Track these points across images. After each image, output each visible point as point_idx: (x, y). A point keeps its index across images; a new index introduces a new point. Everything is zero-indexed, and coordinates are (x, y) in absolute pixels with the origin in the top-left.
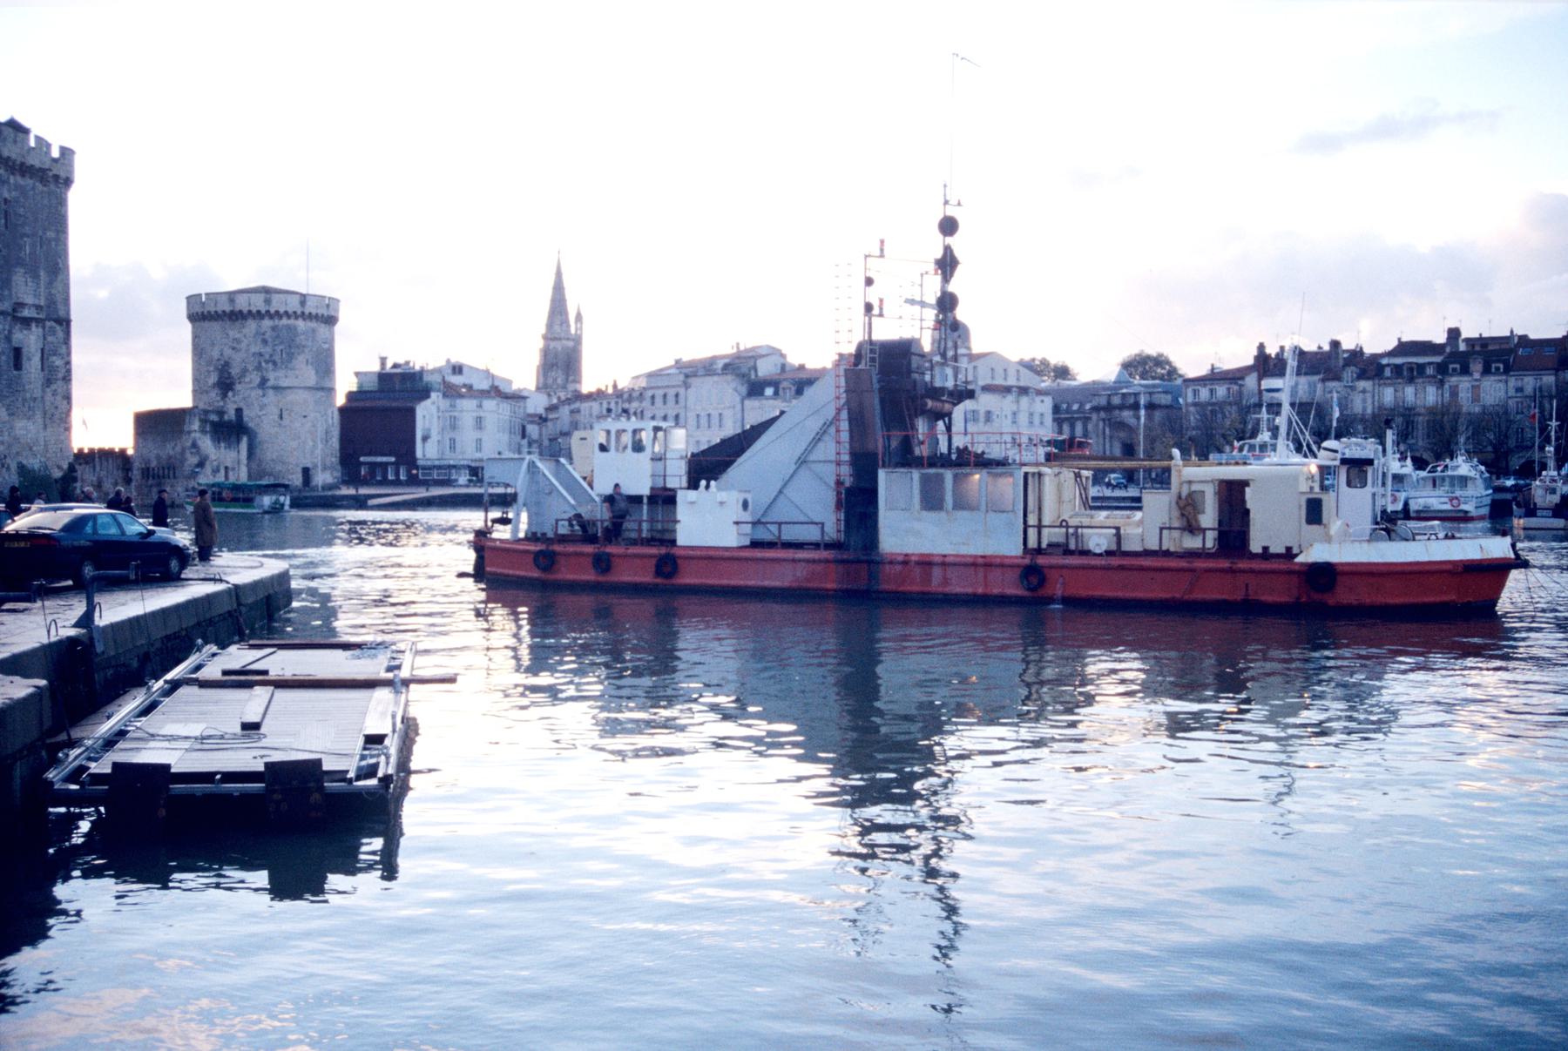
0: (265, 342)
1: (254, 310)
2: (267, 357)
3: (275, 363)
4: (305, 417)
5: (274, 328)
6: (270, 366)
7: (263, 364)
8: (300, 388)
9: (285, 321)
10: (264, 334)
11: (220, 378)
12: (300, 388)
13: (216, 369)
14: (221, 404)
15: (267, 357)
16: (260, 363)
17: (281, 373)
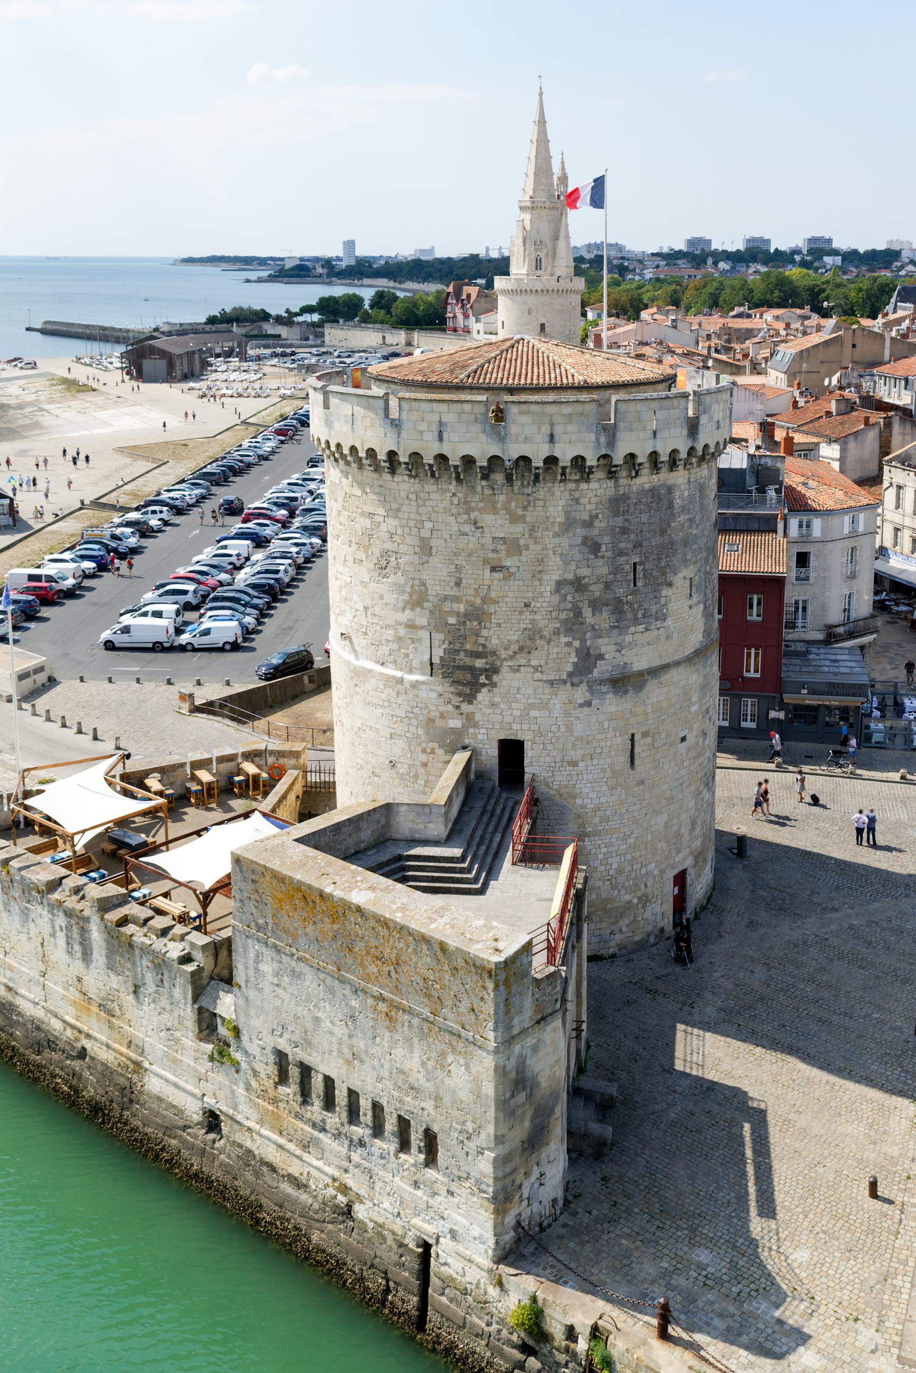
0: (594, 548)
1: (565, 454)
2: (596, 590)
3: (618, 607)
4: (683, 739)
5: (617, 504)
6: (604, 619)
7: (587, 612)
8: (677, 664)
9: (646, 480)
10: (589, 524)
11: (451, 652)
12: (677, 664)
13: (438, 623)
15: (596, 590)
16: (578, 613)
17: (635, 634)
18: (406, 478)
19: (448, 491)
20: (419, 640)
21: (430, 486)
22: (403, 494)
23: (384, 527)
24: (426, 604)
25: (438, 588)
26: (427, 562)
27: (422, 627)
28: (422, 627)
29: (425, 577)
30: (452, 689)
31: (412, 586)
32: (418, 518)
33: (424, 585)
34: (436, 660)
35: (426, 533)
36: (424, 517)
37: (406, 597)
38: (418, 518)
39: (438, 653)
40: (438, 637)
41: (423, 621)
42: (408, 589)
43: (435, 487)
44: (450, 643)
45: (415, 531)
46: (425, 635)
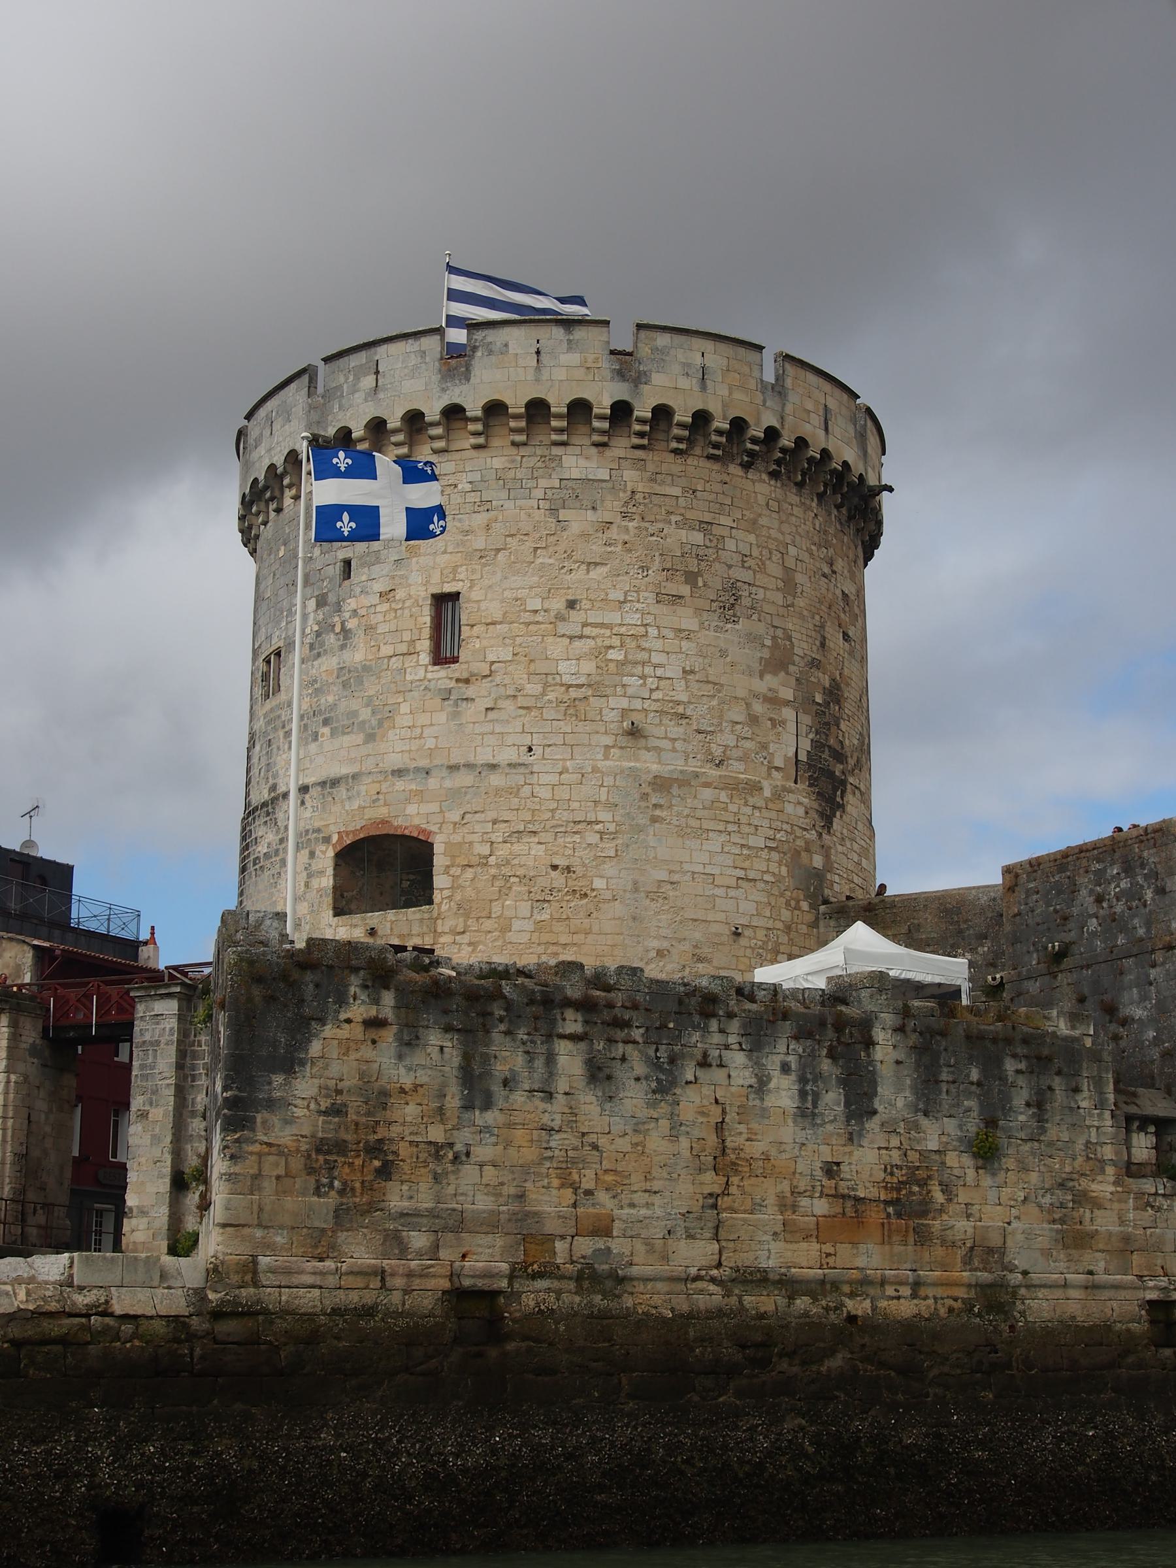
14: (818, 861)
18: (765, 477)
19: (810, 508)
20: (783, 723)
21: (794, 498)
22: (761, 500)
23: (730, 545)
24: (792, 668)
25: (805, 645)
26: (792, 605)
27: (787, 703)
28: (787, 703)
29: (790, 626)
30: (815, 805)
31: (774, 638)
32: (781, 537)
33: (789, 638)
34: (803, 757)
35: (790, 563)
36: (788, 539)
37: (766, 654)
38: (781, 537)
39: (806, 745)
40: (806, 719)
41: (787, 694)
42: (768, 642)
43: (798, 499)
44: (817, 733)
45: (776, 557)
46: (788, 714)
